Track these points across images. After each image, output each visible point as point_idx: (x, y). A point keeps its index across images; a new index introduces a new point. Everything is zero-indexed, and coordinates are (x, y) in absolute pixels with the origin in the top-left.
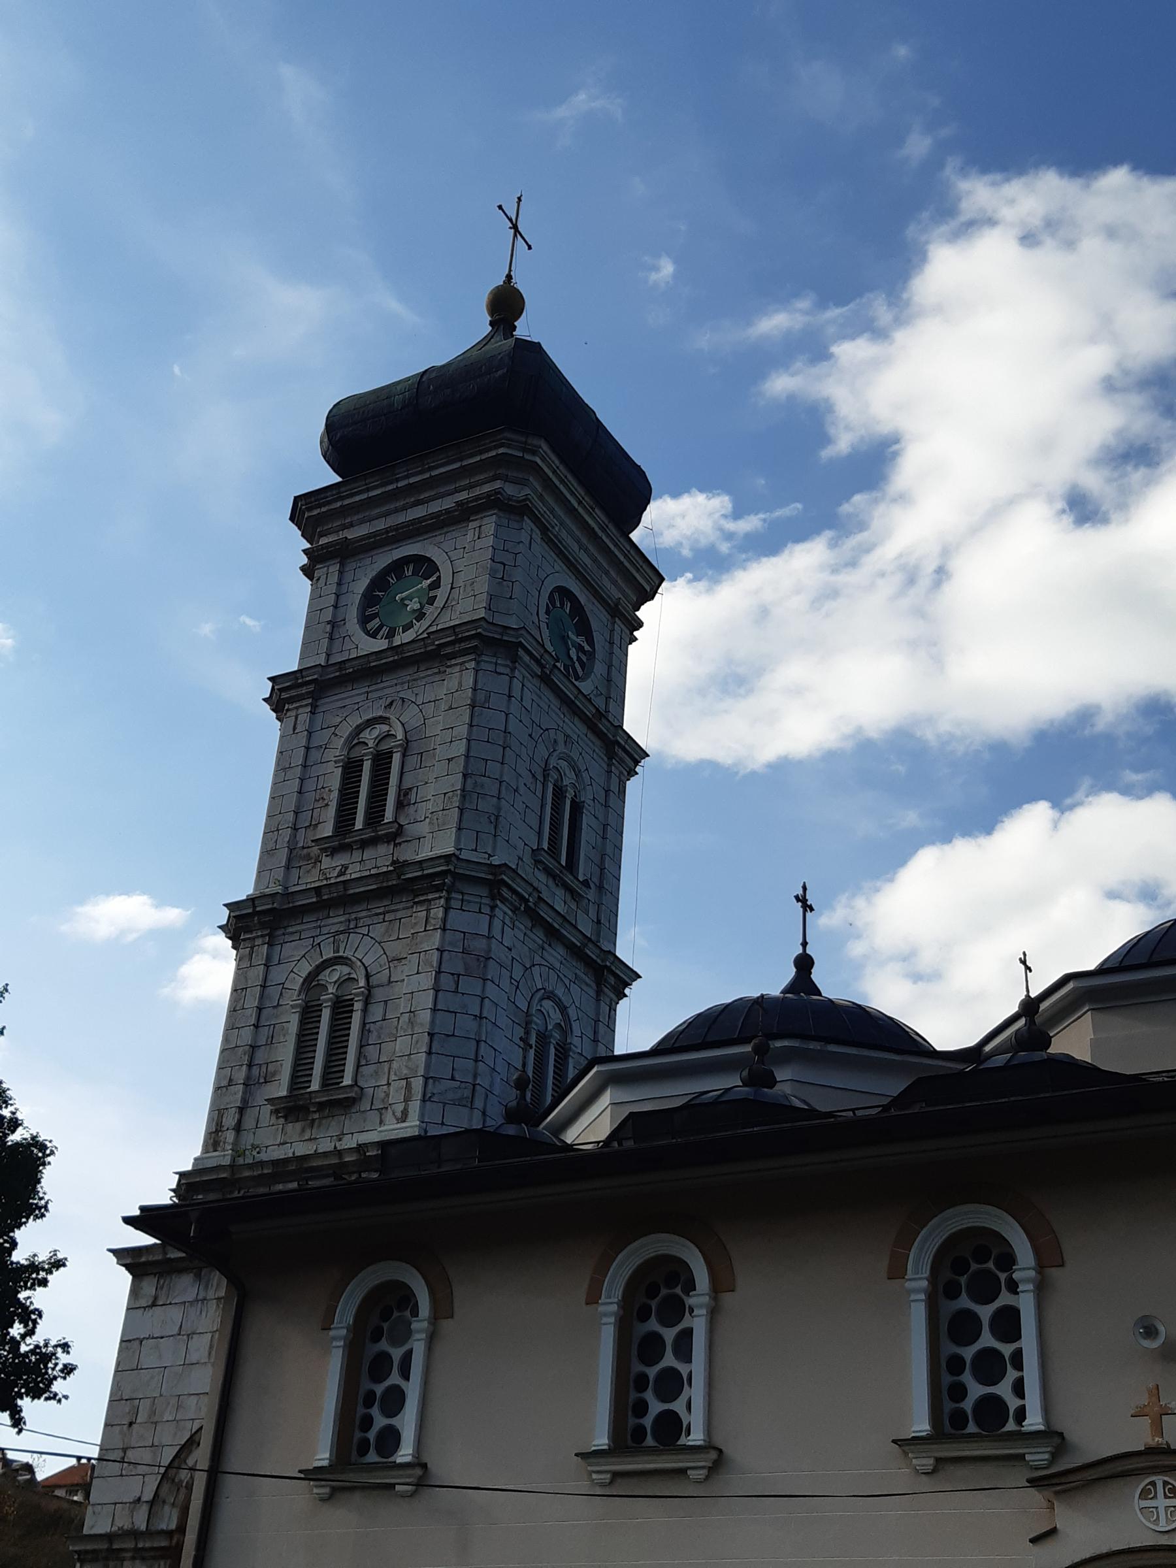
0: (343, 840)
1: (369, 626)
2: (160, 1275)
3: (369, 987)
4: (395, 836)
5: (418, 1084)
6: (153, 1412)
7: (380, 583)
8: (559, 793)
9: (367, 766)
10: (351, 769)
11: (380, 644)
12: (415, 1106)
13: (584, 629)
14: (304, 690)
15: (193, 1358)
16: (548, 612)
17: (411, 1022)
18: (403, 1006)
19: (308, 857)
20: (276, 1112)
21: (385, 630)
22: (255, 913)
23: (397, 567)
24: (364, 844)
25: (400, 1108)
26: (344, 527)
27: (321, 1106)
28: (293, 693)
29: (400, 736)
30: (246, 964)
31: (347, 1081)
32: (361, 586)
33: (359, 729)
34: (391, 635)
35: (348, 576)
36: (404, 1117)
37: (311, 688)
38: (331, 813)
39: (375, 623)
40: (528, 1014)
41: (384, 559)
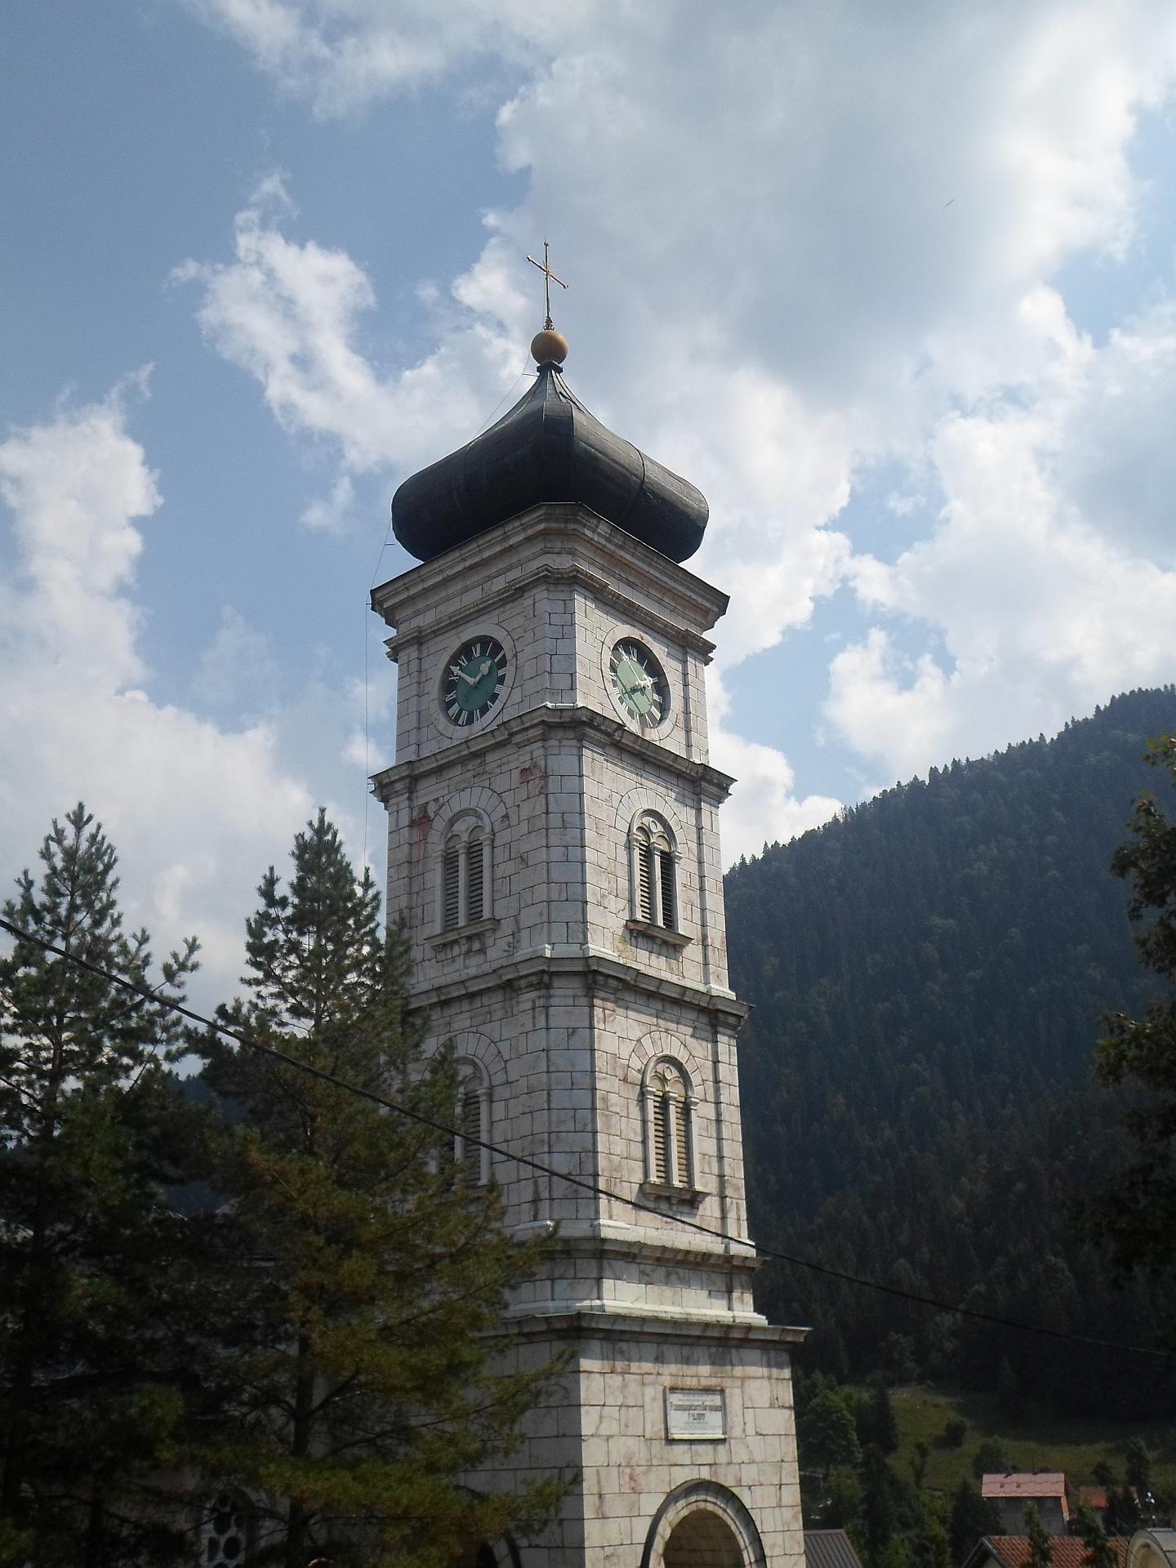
1: (451, 712)
3: (491, 1088)
8: (647, 855)
13: (653, 668)
16: (613, 669)
21: (465, 715)
23: (466, 649)
29: (488, 829)
31: (484, 1181)
32: (437, 674)
33: (452, 822)
34: (470, 721)
35: (426, 665)
39: (456, 708)
40: (643, 1085)
41: (453, 642)
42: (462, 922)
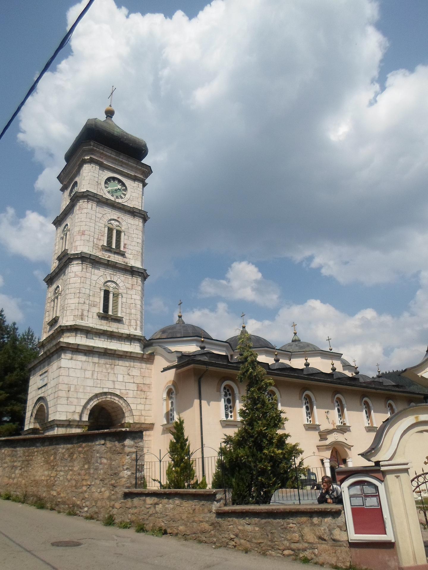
0: (108, 248)
2: (73, 351)
4: (123, 255)
5: (139, 322)
6: (76, 389)
7: (109, 180)
9: (115, 232)
10: (110, 230)
11: (112, 199)
12: (138, 328)
14: (95, 199)
15: (87, 376)
17: (135, 307)
18: (133, 301)
19: (98, 247)
20: (99, 316)
22: (89, 258)
23: (114, 179)
24: (115, 253)
25: (135, 327)
26: (100, 157)
27: (112, 319)
28: (92, 198)
30: (85, 270)
33: (111, 220)
36: (136, 329)
37: (98, 200)
38: (106, 239)
42: (114, 246)
